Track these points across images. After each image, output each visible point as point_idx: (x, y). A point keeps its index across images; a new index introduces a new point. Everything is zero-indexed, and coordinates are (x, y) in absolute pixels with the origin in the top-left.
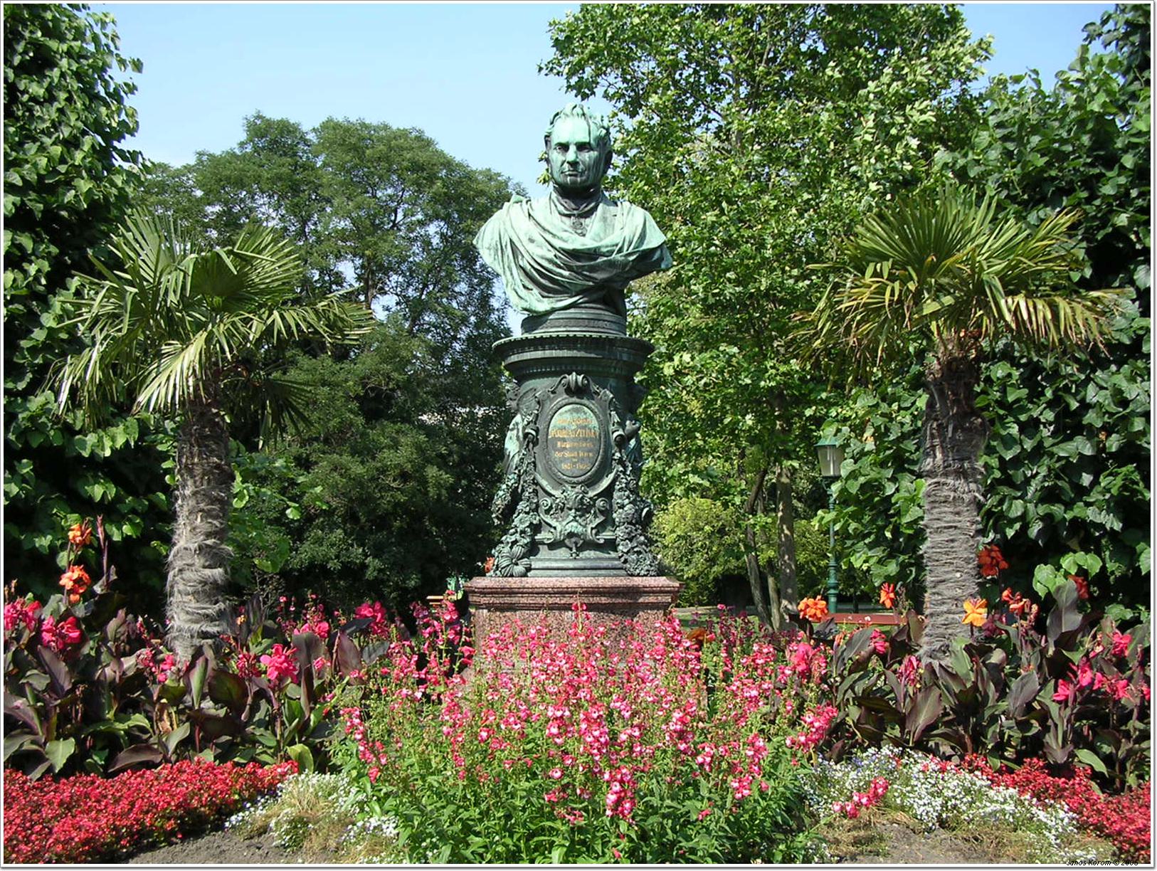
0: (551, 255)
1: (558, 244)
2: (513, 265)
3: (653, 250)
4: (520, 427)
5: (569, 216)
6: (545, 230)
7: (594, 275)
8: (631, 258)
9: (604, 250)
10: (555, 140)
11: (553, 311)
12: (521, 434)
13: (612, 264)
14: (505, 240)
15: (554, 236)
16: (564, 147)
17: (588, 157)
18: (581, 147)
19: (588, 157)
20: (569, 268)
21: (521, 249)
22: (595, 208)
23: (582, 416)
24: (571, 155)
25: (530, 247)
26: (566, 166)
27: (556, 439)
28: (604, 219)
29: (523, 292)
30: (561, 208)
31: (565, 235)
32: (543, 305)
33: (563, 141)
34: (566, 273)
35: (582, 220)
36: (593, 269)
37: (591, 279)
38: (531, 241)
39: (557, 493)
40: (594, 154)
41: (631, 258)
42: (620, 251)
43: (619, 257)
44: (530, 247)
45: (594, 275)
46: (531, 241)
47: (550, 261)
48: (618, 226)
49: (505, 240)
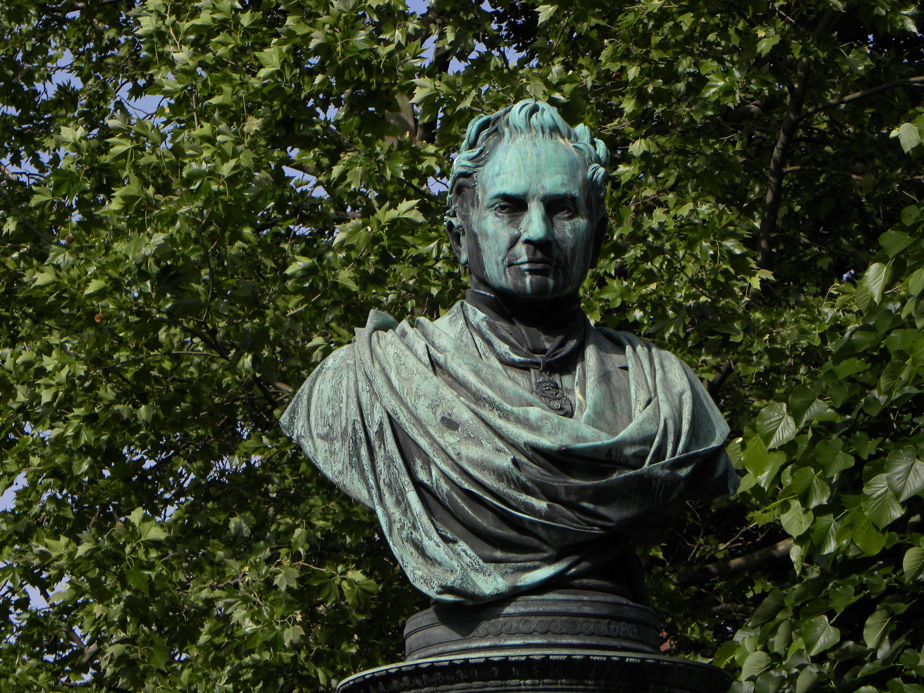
0: (504, 461)
1: (524, 436)
2: (406, 479)
5: (524, 367)
6: (478, 398)
7: (602, 510)
8: (684, 472)
9: (629, 451)
11: (514, 594)
15: (505, 415)
16: (513, 205)
17: (569, 228)
18: (554, 206)
19: (569, 228)
20: (549, 494)
21: (423, 442)
22: (578, 355)
24: (534, 224)
25: (449, 440)
26: (522, 252)
28: (605, 377)
29: (434, 546)
30: (504, 348)
31: (534, 413)
32: (490, 583)
33: (509, 189)
34: (542, 505)
35: (556, 378)
36: (600, 496)
38: (450, 424)
40: (581, 222)
41: (684, 472)
42: (660, 454)
44: (449, 440)
45: (602, 510)
46: (450, 424)
47: (500, 474)
48: (637, 396)
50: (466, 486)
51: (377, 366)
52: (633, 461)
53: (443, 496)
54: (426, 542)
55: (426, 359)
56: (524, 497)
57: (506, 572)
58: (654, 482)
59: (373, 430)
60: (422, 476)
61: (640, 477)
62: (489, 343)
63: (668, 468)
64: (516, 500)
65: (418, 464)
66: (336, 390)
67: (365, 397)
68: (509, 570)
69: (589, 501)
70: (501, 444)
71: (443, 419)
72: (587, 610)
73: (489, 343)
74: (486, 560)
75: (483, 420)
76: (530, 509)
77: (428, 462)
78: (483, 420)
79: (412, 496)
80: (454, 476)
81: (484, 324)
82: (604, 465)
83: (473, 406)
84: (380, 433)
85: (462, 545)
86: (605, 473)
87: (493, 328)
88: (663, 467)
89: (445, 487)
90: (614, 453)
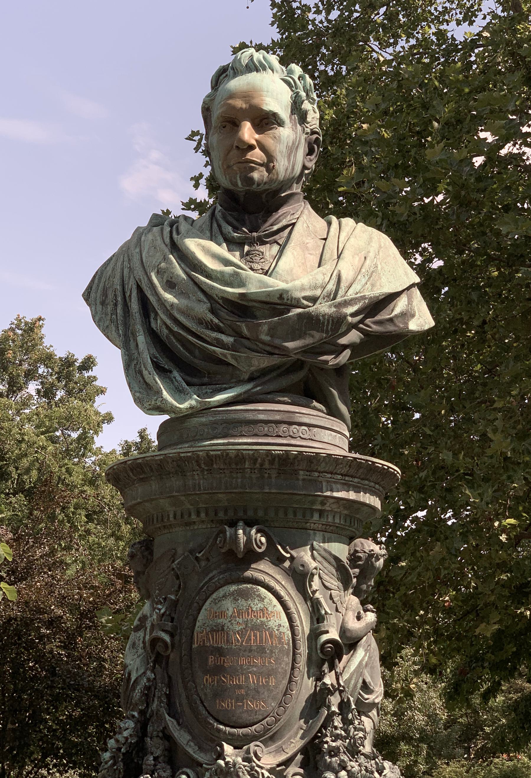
3: (393, 297)
4: (148, 625)
10: (217, 112)
12: (147, 637)
13: (311, 322)
14: (131, 284)
21: (152, 299)
23: (257, 605)
25: (168, 297)
27: (205, 650)
31: (229, 269)
37: (272, 350)
39: (200, 757)
43: (324, 308)
49: (131, 284)
50: (176, 329)
51: (138, 250)
52: (305, 302)
53: (164, 338)
54: (145, 373)
55: (167, 240)
56: (214, 335)
57: (206, 392)
58: (321, 318)
59: (128, 295)
60: (153, 325)
61: (309, 315)
62: (219, 226)
63: (335, 306)
64: (209, 337)
65: (152, 315)
66: (113, 269)
67: (126, 271)
68: (208, 391)
69: (267, 335)
70: (201, 296)
71: (168, 281)
72: (262, 417)
73: (219, 226)
74: (189, 384)
75: (193, 280)
76: (220, 344)
77: (156, 314)
78: (193, 280)
79: (141, 339)
80: (168, 322)
81: (220, 214)
82: (279, 307)
83: (188, 270)
84: (130, 296)
85: (176, 374)
86: (282, 313)
87: (224, 218)
88: (330, 306)
89: (165, 331)
90: (285, 296)
